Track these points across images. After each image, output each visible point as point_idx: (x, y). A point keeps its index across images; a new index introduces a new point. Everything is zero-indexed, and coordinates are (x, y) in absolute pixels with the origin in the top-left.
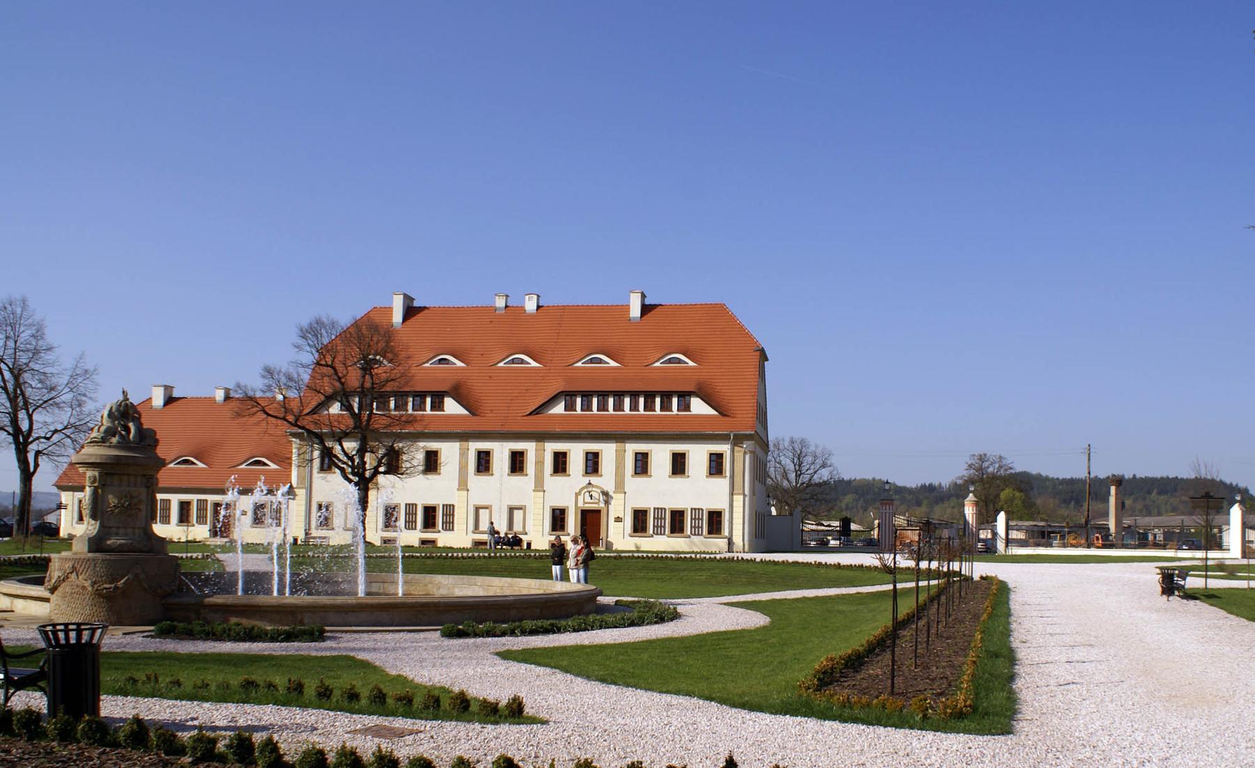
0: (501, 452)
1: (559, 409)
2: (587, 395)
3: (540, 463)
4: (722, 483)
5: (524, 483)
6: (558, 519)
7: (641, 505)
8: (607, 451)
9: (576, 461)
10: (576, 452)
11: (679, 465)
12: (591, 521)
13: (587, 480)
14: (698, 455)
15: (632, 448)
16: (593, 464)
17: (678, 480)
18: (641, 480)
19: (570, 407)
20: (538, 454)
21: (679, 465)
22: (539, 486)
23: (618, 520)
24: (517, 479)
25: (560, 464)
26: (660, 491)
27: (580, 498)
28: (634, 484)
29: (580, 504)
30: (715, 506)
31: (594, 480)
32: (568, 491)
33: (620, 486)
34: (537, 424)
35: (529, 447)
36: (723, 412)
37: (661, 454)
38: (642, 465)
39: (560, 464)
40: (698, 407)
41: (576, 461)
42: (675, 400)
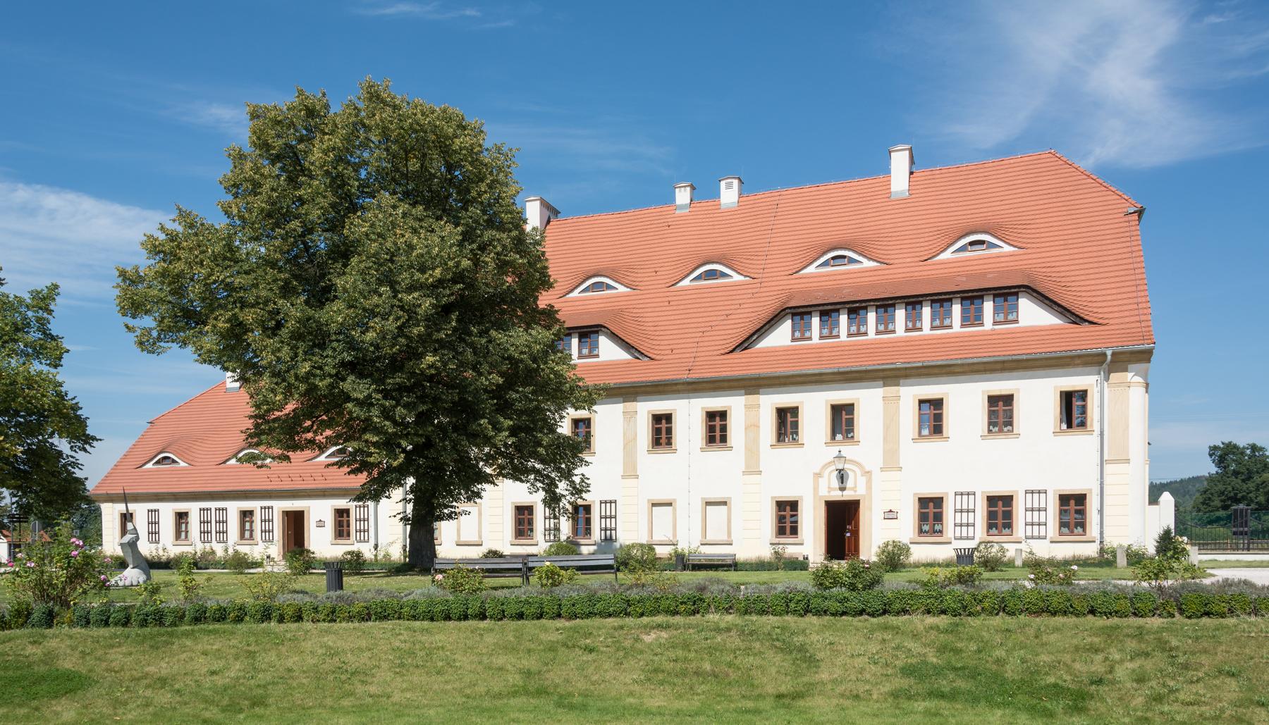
0: (689, 414)
1: (781, 336)
4: (1081, 444)
6: (787, 515)
7: (930, 491)
8: (868, 402)
10: (814, 407)
11: (1001, 412)
12: (842, 520)
13: (834, 451)
14: (1037, 397)
15: (910, 394)
16: (842, 419)
17: (1001, 443)
18: (933, 446)
19: (801, 332)
20: (751, 414)
21: (1001, 412)
22: (752, 470)
23: (891, 515)
24: (717, 456)
25: (787, 422)
26: (968, 462)
27: (823, 483)
31: (848, 450)
33: (891, 463)
34: (741, 365)
35: (734, 404)
36: (1075, 318)
37: (965, 401)
38: (933, 417)
39: (787, 422)
40: (1030, 314)
42: (988, 306)
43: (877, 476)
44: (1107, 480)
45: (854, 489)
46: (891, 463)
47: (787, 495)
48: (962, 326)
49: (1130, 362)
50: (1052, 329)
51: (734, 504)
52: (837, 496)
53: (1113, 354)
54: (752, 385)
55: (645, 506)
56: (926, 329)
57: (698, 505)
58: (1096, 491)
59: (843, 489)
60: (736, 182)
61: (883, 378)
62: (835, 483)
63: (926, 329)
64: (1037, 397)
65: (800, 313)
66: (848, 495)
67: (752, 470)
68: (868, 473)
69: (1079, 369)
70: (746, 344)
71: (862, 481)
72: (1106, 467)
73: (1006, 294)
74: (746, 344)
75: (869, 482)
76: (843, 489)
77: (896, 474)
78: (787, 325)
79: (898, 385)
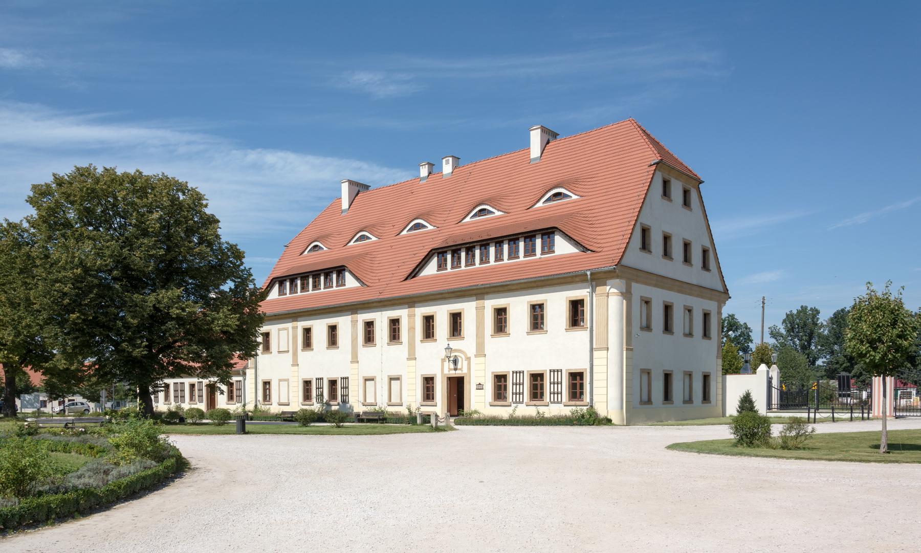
1: (431, 269)
2: (455, 251)
3: (412, 329)
4: (581, 336)
5: (400, 350)
7: (501, 370)
9: (442, 326)
14: (556, 304)
20: (411, 319)
22: (412, 357)
23: (480, 387)
24: (395, 348)
27: (446, 364)
28: (494, 344)
29: (446, 371)
30: (576, 367)
32: (432, 358)
33: (481, 353)
35: (402, 313)
36: (585, 249)
37: (518, 308)
40: (562, 247)
41: (442, 326)
43: (473, 360)
44: (595, 363)
45: (461, 369)
46: (481, 353)
47: (429, 373)
48: (525, 256)
49: (607, 278)
50: (571, 256)
51: (404, 379)
52: (453, 374)
53: (591, 274)
54: (411, 301)
55: (362, 381)
56: (506, 260)
57: (386, 380)
58: (588, 370)
59: (456, 369)
60: (451, 159)
61: (476, 295)
62: (452, 366)
63: (506, 260)
64: (556, 304)
65: (440, 252)
66: (458, 373)
67: (412, 357)
68: (468, 359)
69: (580, 285)
70: (414, 274)
71: (465, 363)
72: (595, 353)
73: (548, 233)
74: (414, 274)
75: (469, 364)
76: (456, 369)
77: (481, 359)
78: (434, 262)
79: (483, 299)
